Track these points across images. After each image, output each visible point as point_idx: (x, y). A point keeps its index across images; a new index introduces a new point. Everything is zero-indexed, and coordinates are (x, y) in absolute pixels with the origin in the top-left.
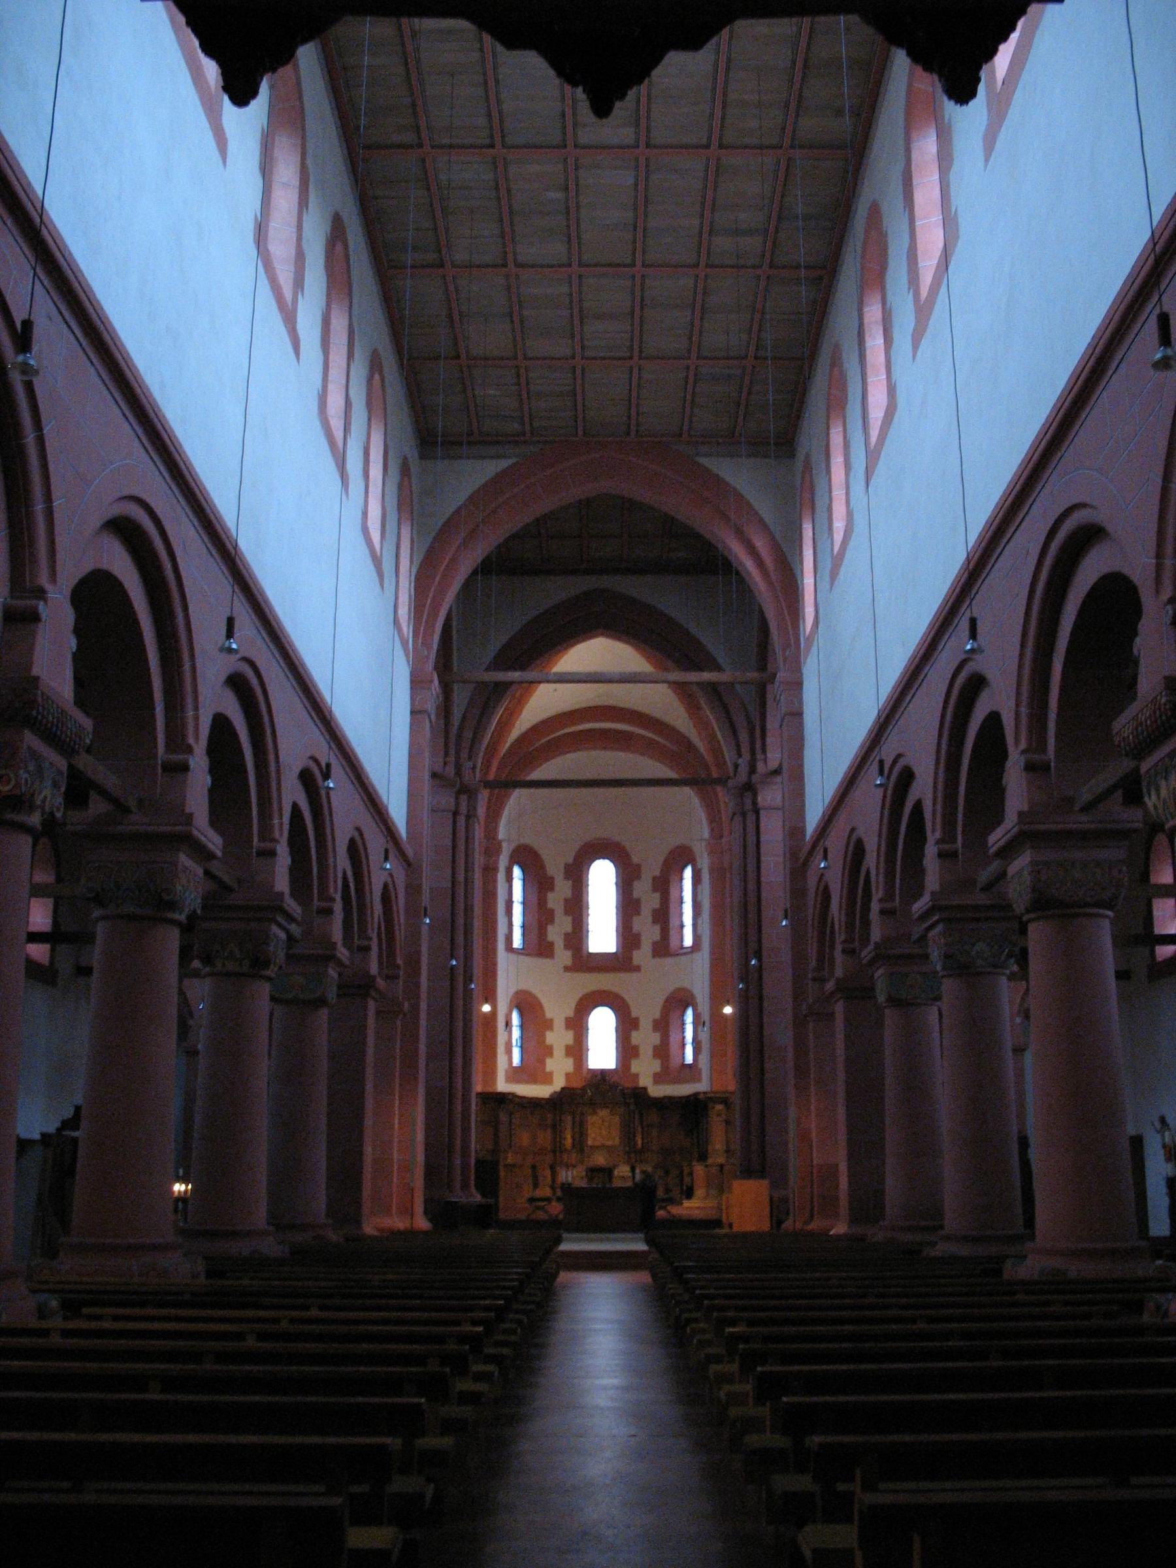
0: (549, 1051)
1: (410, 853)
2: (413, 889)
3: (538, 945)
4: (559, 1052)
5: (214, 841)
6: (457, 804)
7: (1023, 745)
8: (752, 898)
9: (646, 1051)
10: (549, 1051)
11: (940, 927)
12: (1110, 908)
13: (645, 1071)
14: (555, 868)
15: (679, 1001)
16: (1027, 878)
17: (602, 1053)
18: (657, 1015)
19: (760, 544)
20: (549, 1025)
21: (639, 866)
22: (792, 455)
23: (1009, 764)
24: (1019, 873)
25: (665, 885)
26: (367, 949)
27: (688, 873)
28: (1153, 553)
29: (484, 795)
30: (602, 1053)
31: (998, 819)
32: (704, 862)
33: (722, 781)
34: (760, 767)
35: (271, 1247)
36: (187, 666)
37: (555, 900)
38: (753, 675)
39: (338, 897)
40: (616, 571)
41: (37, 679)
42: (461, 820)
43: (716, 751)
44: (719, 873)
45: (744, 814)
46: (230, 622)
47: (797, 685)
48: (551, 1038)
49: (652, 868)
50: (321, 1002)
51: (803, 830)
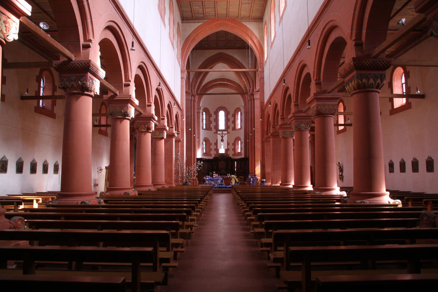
0: (211, 150)
1: (181, 108)
2: (182, 116)
3: (208, 128)
4: (213, 150)
5: (137, 102)
6: (191, 99)
7: (315, 78)
8: (253, 118)
9: (231, 150)
10: (211, 150)
11: (294, 121)
12: (334, 115)
13: (231, 154)
14: (212, 112)
15: (238, 139)
16: (315, 108)
19: (255, 41)
20: (211, 144)
21: (229, 112)
22: (262, 22)
23: (311, 83)
24: (313, 108)
25: (234, 116)
26: (173, 127)
27: (239, 113)
28: (350, 29)
29: (197, 97)
30: (222, 151)
31: (309, 95)
32: (243, 111)
33: (247, 93)
34: (255, 90)
35: (152, 189)
36: (129, 62)
37: (212, 119)
38: (254, 70)
39: (166, 116)
40: (224, 49)
41: (90, 60)
42: (192, 102)
43: (246, 87)
44: (246, 113)
45: (251, 100)
46: (133, 43)
47: (263, 72)
48: (211, 147)
49: (232, 112)
50: (163, 138)
51: (264, 102)
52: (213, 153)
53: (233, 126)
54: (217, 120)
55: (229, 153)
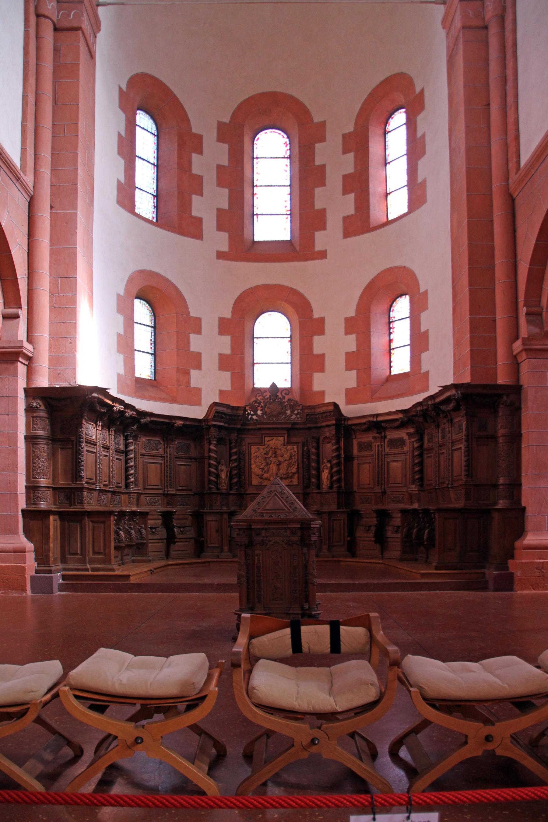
0: (196, 361)
4: (210, 361)
9: (335, 362)
10: (196, 361)
13: (334, 386)
17: (272, 361)
18: (352, 313)
20: (195, 325)
30: (272, 361)
48: (196, 343)
52: (210, 387)
53: (351, 210)
54: (237, 178)
55: (319, 382)
